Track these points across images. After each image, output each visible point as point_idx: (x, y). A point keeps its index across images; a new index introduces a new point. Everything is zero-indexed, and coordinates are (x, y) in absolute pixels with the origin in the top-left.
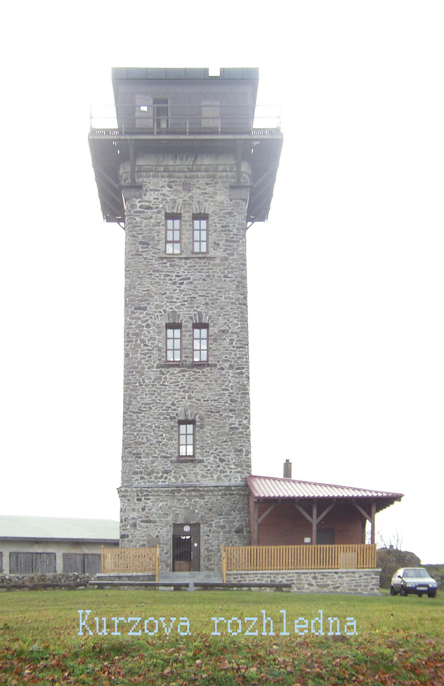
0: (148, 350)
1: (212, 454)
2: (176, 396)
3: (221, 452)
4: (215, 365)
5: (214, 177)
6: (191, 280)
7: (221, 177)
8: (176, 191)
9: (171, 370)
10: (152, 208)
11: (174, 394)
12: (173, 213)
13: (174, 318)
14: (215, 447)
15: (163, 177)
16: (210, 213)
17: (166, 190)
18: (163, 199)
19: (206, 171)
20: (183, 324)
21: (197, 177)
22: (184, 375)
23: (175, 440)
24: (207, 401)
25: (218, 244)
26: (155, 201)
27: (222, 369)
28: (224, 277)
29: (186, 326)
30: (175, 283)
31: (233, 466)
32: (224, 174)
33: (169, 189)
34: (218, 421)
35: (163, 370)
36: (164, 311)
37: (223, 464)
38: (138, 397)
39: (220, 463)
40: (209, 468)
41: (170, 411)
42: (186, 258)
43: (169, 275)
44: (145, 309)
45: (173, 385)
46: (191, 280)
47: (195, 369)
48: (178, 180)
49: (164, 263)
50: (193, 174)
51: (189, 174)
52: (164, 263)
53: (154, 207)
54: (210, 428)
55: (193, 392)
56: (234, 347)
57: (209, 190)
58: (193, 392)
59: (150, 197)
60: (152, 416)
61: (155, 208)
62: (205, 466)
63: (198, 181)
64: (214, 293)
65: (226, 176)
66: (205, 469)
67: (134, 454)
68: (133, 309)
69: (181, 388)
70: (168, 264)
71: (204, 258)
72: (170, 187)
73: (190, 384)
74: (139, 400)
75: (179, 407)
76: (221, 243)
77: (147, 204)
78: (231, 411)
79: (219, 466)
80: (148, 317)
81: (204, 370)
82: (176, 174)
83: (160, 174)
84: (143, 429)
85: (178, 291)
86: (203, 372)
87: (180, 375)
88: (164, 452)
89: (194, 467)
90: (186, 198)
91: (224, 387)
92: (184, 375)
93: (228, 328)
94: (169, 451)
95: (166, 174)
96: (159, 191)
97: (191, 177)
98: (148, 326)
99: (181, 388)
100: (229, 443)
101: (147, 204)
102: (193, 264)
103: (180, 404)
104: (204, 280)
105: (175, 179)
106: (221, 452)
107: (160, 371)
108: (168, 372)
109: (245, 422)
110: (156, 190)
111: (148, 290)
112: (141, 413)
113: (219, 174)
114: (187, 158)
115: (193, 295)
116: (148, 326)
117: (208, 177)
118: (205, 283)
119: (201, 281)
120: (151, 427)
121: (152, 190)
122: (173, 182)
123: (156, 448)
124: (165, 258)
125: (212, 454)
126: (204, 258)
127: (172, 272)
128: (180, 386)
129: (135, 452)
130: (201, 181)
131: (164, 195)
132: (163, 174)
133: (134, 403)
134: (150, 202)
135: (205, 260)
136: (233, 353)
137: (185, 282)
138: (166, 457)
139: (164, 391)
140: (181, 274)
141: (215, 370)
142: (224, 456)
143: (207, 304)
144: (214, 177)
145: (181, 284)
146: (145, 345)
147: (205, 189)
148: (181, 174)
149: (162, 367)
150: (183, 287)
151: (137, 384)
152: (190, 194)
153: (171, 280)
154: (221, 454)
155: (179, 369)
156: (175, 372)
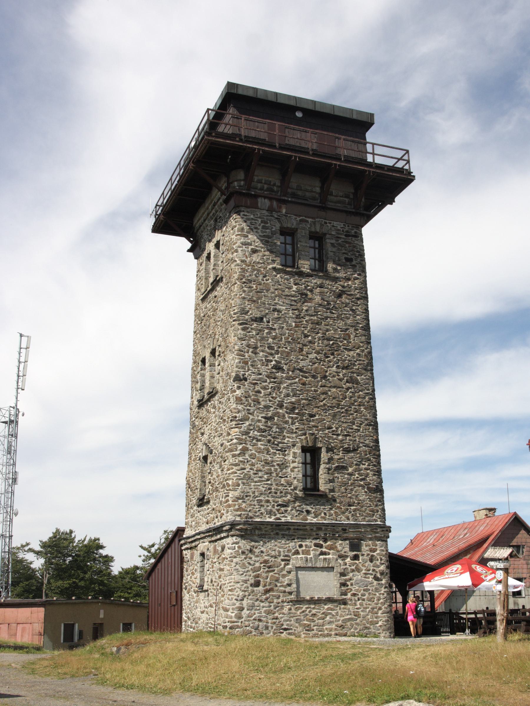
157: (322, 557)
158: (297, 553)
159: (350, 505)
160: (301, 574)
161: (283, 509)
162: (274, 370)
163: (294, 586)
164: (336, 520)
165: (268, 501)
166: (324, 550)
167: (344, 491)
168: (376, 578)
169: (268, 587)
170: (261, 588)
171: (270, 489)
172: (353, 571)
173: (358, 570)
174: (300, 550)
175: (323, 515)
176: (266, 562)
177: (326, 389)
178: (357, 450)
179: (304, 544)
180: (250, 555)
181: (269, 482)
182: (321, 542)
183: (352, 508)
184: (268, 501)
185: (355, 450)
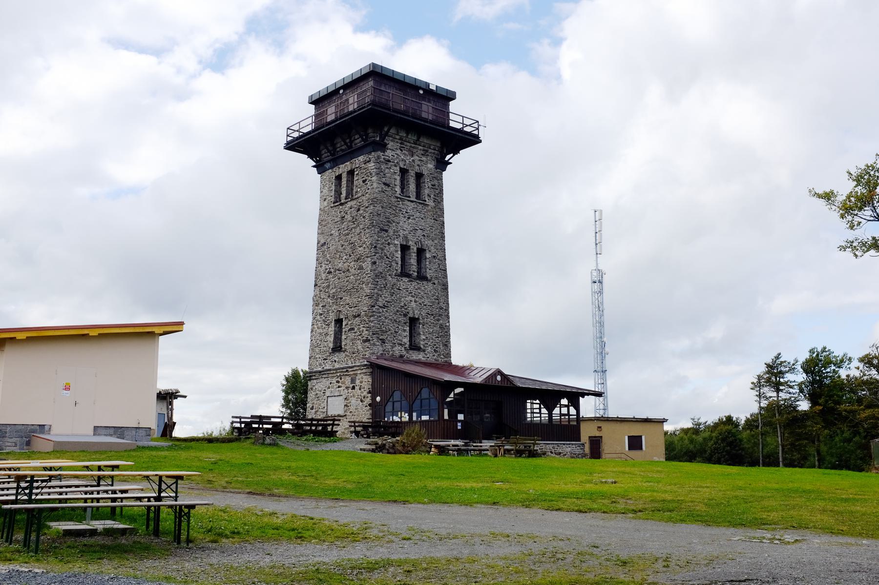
0: (389, 261)
1: (430, 345)
2: (407, 299)
3: (435, 345)
4: (430, 281)
5: (427, 151)
6: (414, 217)
7: (431, 153)
8: (405, 154)
9: (404, 279)
10: (390, 162)
11: (406, 297)
12: (404, 168)
13: (406, 242)
14: (431, 341)
15: (397, 142)
16: (426, 174)
17: (399, 152)
18: (397, 158)
19: (423, 146)
20: (411, 247)
21: (417, 148)
22: (411, 284)
23: (407, 332)
24: (426, 305)
25: (430, 196)
26: (392, 157)
27: (434, 284)
28: (434, 219)
29: (413, 249)
30: (405, 217)
31: (442, 356)
32: (433, 151)
33: (400, 152)
34: (432, 321)
35: (398, 278)
36: (399, 236)
37: (436, 355)
38: (383, 296)
39: (435, 353)
40: (428, 356)
41: (403, 309)
42: (412, 201)
43: (401, 211)
44: (386, 231)
45: (404, 291)
46: (414, 217)
47: (418, 281)
48: (406, 147)
49: (398, 201)
50: (416, 146)
51: (413, 145)
52: (398, 201)
53: (392, 161)
54: (428, 326)
55: (417, 297)
56: (440, 269)
57: (424, 158)
58: (417, 297)
59: (389, 153)
60: (392, 311)
61: (392, 162)
62: (426, 355)
63: (417, 151)
64: (428, 229)
65: (434, 153)
66: (425, 356)
67: (381, 340)
68: (379, 230)
69: (410, 293)
70: (401, 203)
71: (422, 203)
72: (402, 151)
73: (415, 292)
74: (383, 298)
75: (409, 307)
76: (432, 196)
77: (388, 158)
78: (440, 315)
79: (434, 356)
80: (388, 238)
81: (423, 282)
82: (405, 143)
83: (396, 140)
84: (386, 321)
85: (407, 223)
86: (423, 284)
87: (409, 283)
88: (400, 340)
89: (419, 354)
90: (411, 161)
91: (435, 297)
92: (411, 284)
93: (436, 255)
94: (404, 340)
95: (400, 141)
96: (394, 151)
97: (413, 148)
98: (389, 244)
99: (410, 293)
100: (440, 339)
101: (388, 158)
102: (415, 206)
103: (409, 305)
104: (422, 219)
105: (404, 146)
106: (435, 345)
107: (397, 278)
108: (402, 280)
109: (448, 324)
110: (393, 150)
111: (389, 218)
112: (385, 308)
113: (430, 151)
114: (414, 135)
115: (416, 228)
116: (389, 244)
117: (423, 150)
118: (423, 221)
119: (420, 219)
120: (391, 320)
121: (390, 149)
122: (403, 147)
123: (395, 337)
124: (399, 198)
125: (430, 345)
126: (422, 203)
127: (403, 209)
128: (409, 292)
129: (381, 338)
130: (419, 152)
131: (398, 155)
132: (397, 140)
133: (380, 300)
134: (389, 157)
135: (422, 205)
136: (440, 274)
137: (411, 218)
138: (401, 345)
139: (399, 294)
140: (408, 211)
141: (430, 284)
142: (437, 348)
143: (424, 235)
144: (427, 151)
145: (409, 218)
146: (387, 257)
147: (421, 157)
148: (408, 144)
149: (398, 276)
150: (410, 220)
151: (382, 286)
152: (413, 159)
153: (402, 214)
154: (435, 347)
155: (408, 279)
156: (406, 281)
157: (338, 389)
158: (329, 388)
159: (353, 354)
160: (330, 401)
161: (325, 361)
162: (328, 275)
163: (326, 408)
164: (347, 364)
165: (320, 358)
166: (340, 384)
167: (351, 344)
168: (362, 401)
169: (317, 410)
170: (314, 410)
171: (320, 350)
172: (351, 397)
173: (354, 396)
174: (330, 386)
175: (341, 362)
176: (317, 394)
177: (348, 278)
178: (360, 315)
179: (332, 382)
180: (312, 391)
181: (320, 346)
182: (339, 380)
183: (354, 355)
184: (320, 358)
185: (359, 315)
